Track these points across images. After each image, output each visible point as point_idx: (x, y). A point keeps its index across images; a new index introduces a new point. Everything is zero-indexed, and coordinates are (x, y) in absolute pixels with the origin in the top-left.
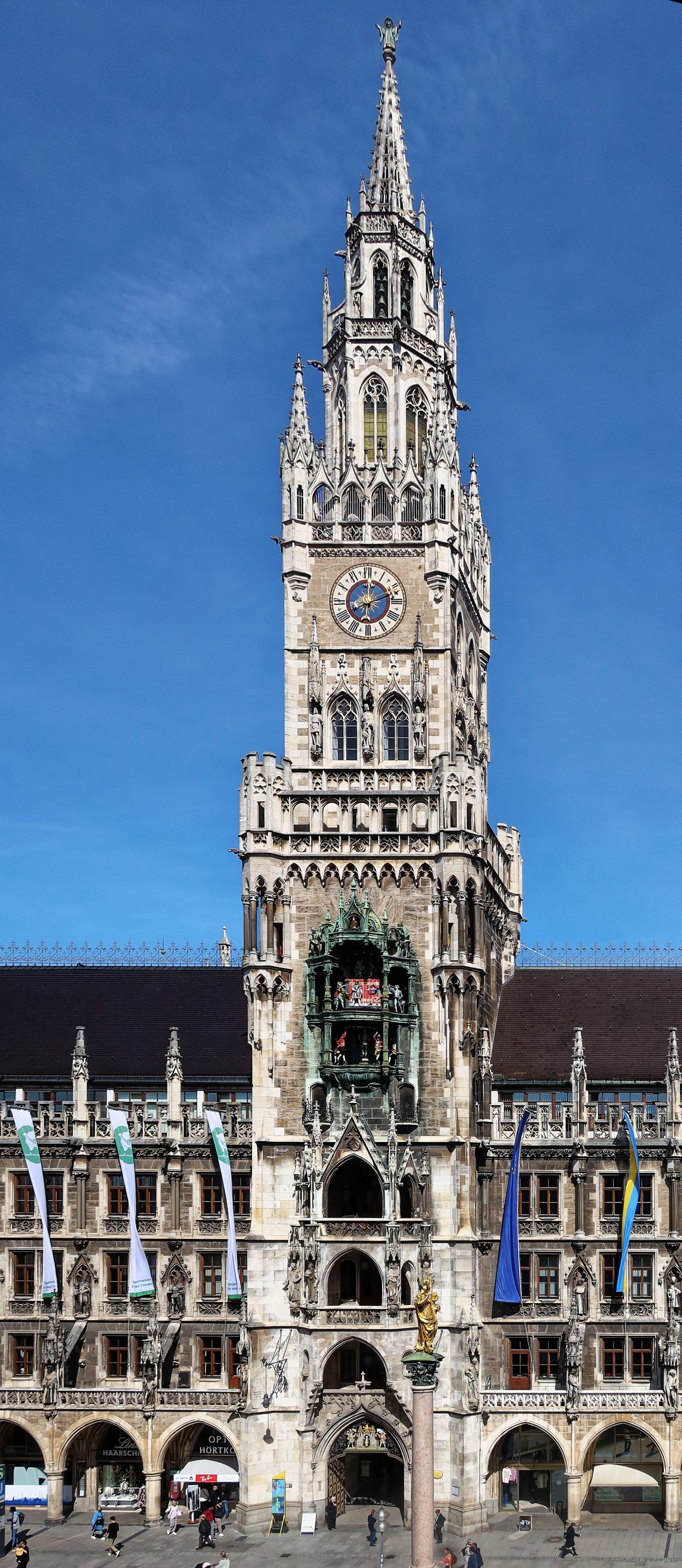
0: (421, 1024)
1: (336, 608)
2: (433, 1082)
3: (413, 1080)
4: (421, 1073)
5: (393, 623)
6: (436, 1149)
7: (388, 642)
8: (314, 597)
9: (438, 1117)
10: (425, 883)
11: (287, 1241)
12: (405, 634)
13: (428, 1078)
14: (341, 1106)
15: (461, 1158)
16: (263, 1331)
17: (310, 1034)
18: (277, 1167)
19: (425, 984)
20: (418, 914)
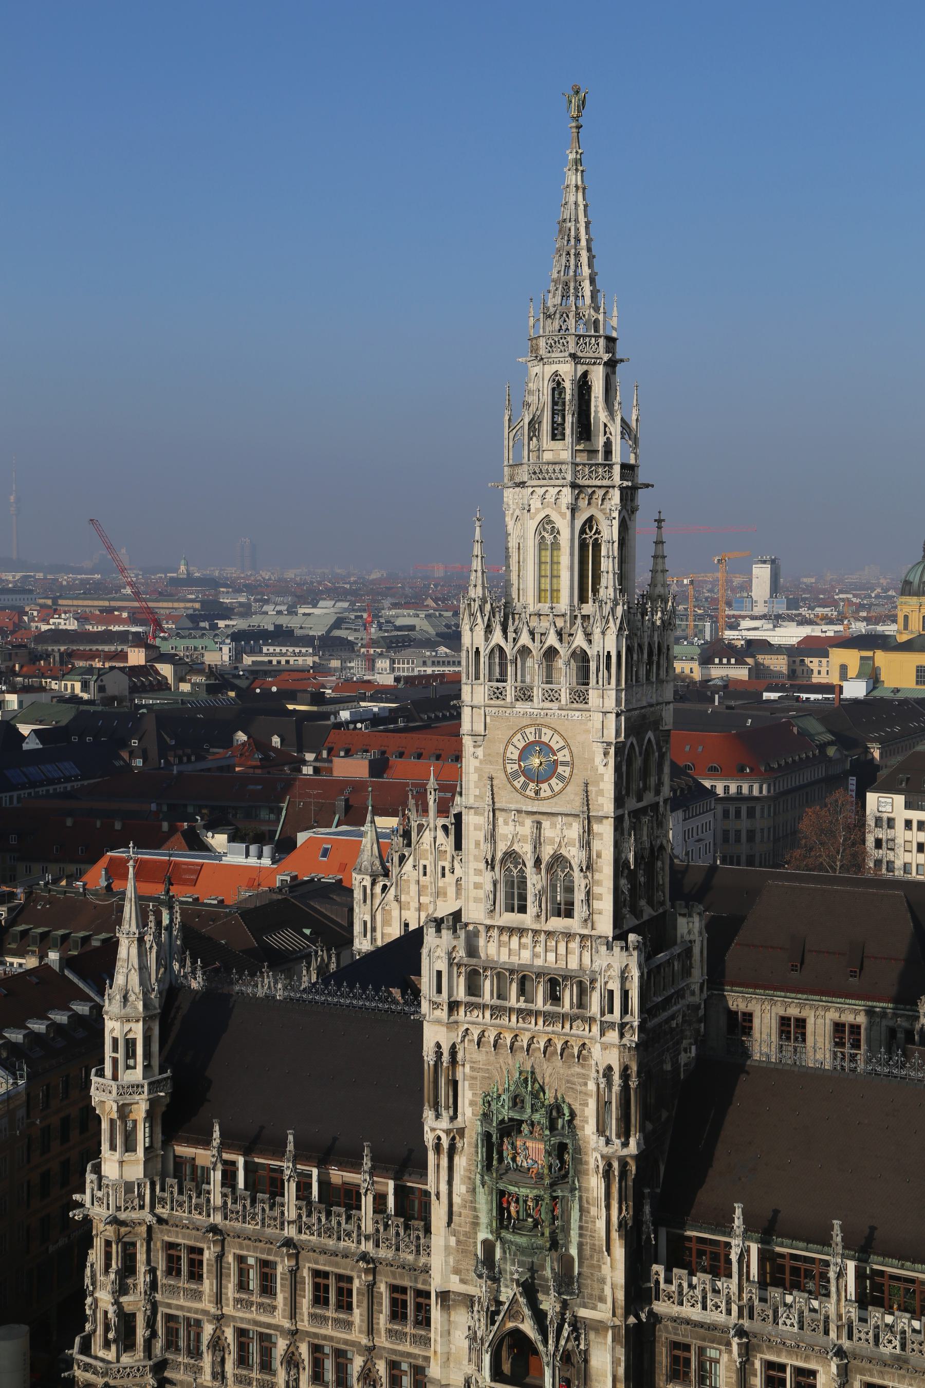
0: (580, 1198)
1: (508, 766)
2: (592, 1256)
3: (574, 1252)
4: (580, 1246)
5: (561, 785)
7: (556, 803)
8: (489, 755)
9: (596, 1293)
12: (572, 797)
13: (587, 1251)
17: (481, 1190)
18: (453, 1313)
19: (585, 1158)
20: (578, 1088)
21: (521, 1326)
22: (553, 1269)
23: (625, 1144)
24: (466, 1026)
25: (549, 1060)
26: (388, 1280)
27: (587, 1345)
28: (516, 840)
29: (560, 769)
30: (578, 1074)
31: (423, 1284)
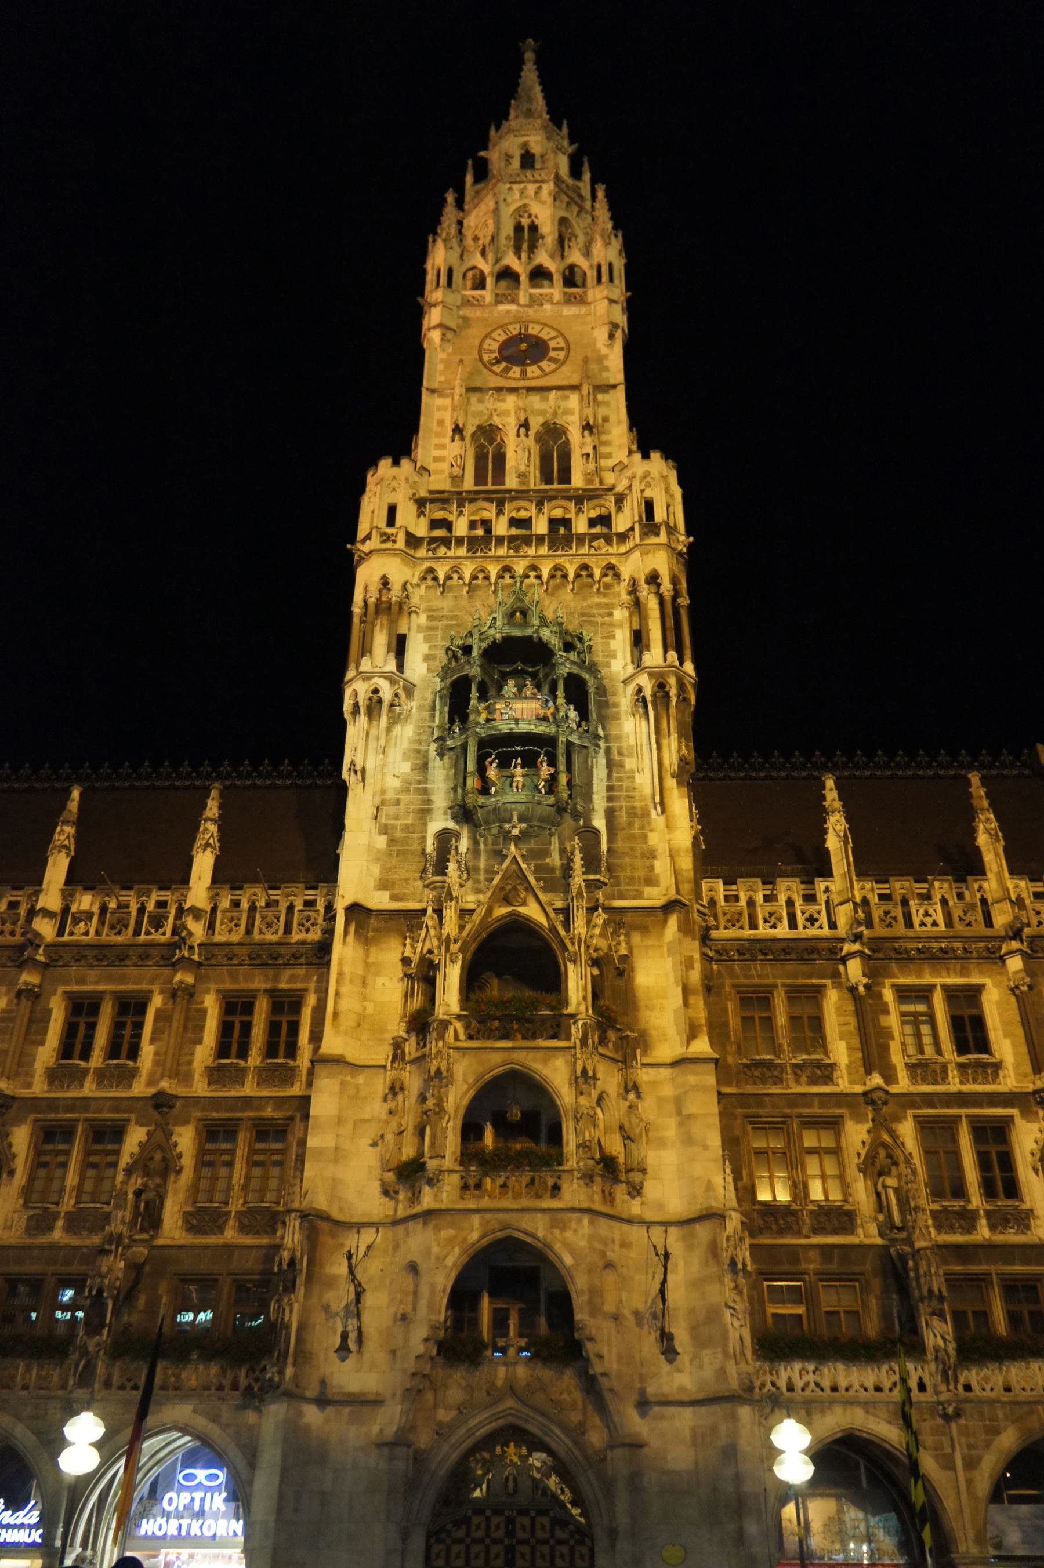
0: (608, 751)
2: (630, 825)
3: (599, 822)
4: (610, 815)
5: (553, 366)
6: (639, 919)
10: (607, 586)
11: (385, 1067)
14: (483, 858)
15: (685, 928)
16: (324, 1226)
18: (373, 950)
19: (612, 699)
20: (599, 620)
21: (522, 910)
22: (562, 851)
23: (681, 661)
24: (427, 565)
25: (552, 594)
26: (221, 986)
27: (630, 949)
28: (494, 414)
29: (552, 354)
30: (599, 605)
31: (289, 982)
